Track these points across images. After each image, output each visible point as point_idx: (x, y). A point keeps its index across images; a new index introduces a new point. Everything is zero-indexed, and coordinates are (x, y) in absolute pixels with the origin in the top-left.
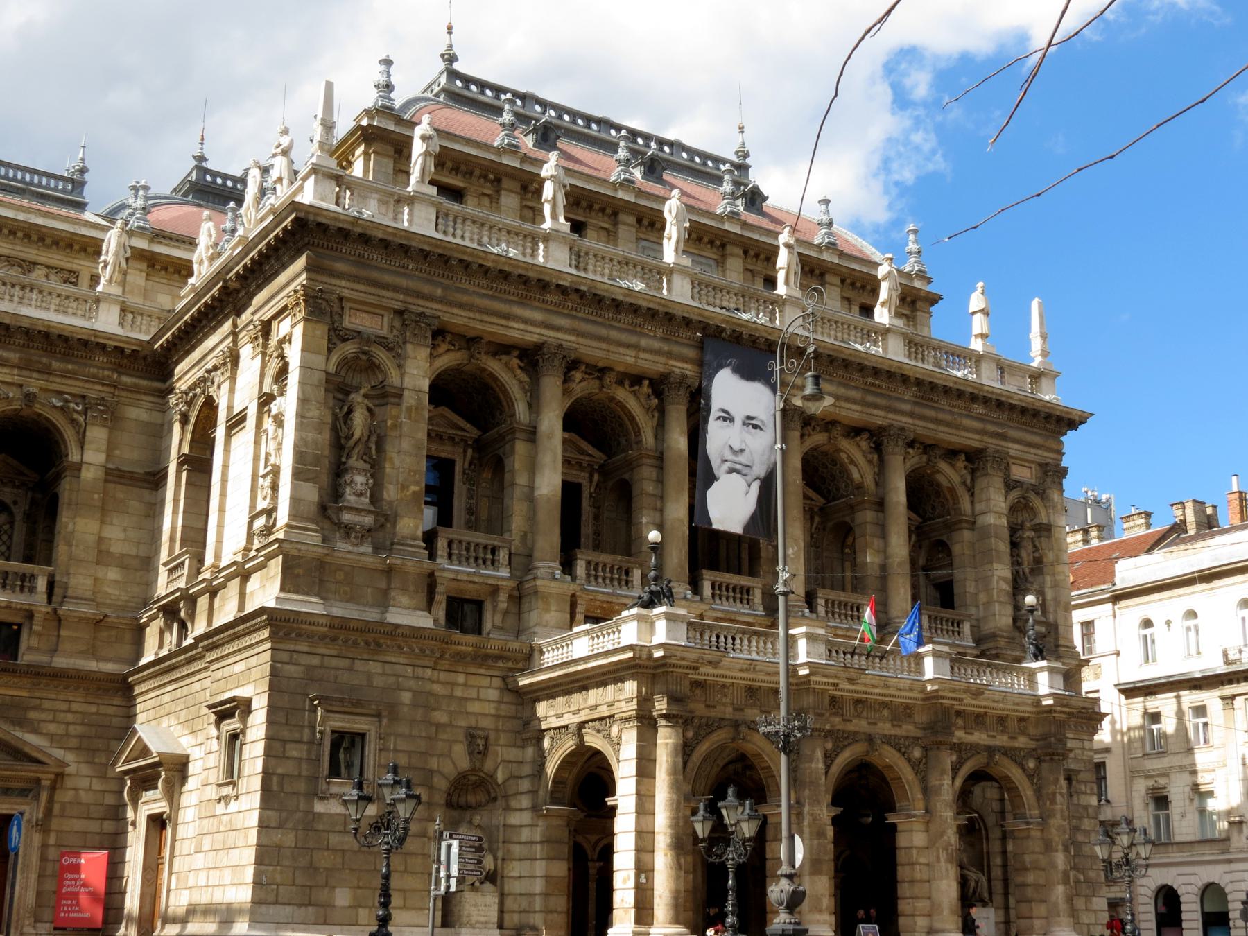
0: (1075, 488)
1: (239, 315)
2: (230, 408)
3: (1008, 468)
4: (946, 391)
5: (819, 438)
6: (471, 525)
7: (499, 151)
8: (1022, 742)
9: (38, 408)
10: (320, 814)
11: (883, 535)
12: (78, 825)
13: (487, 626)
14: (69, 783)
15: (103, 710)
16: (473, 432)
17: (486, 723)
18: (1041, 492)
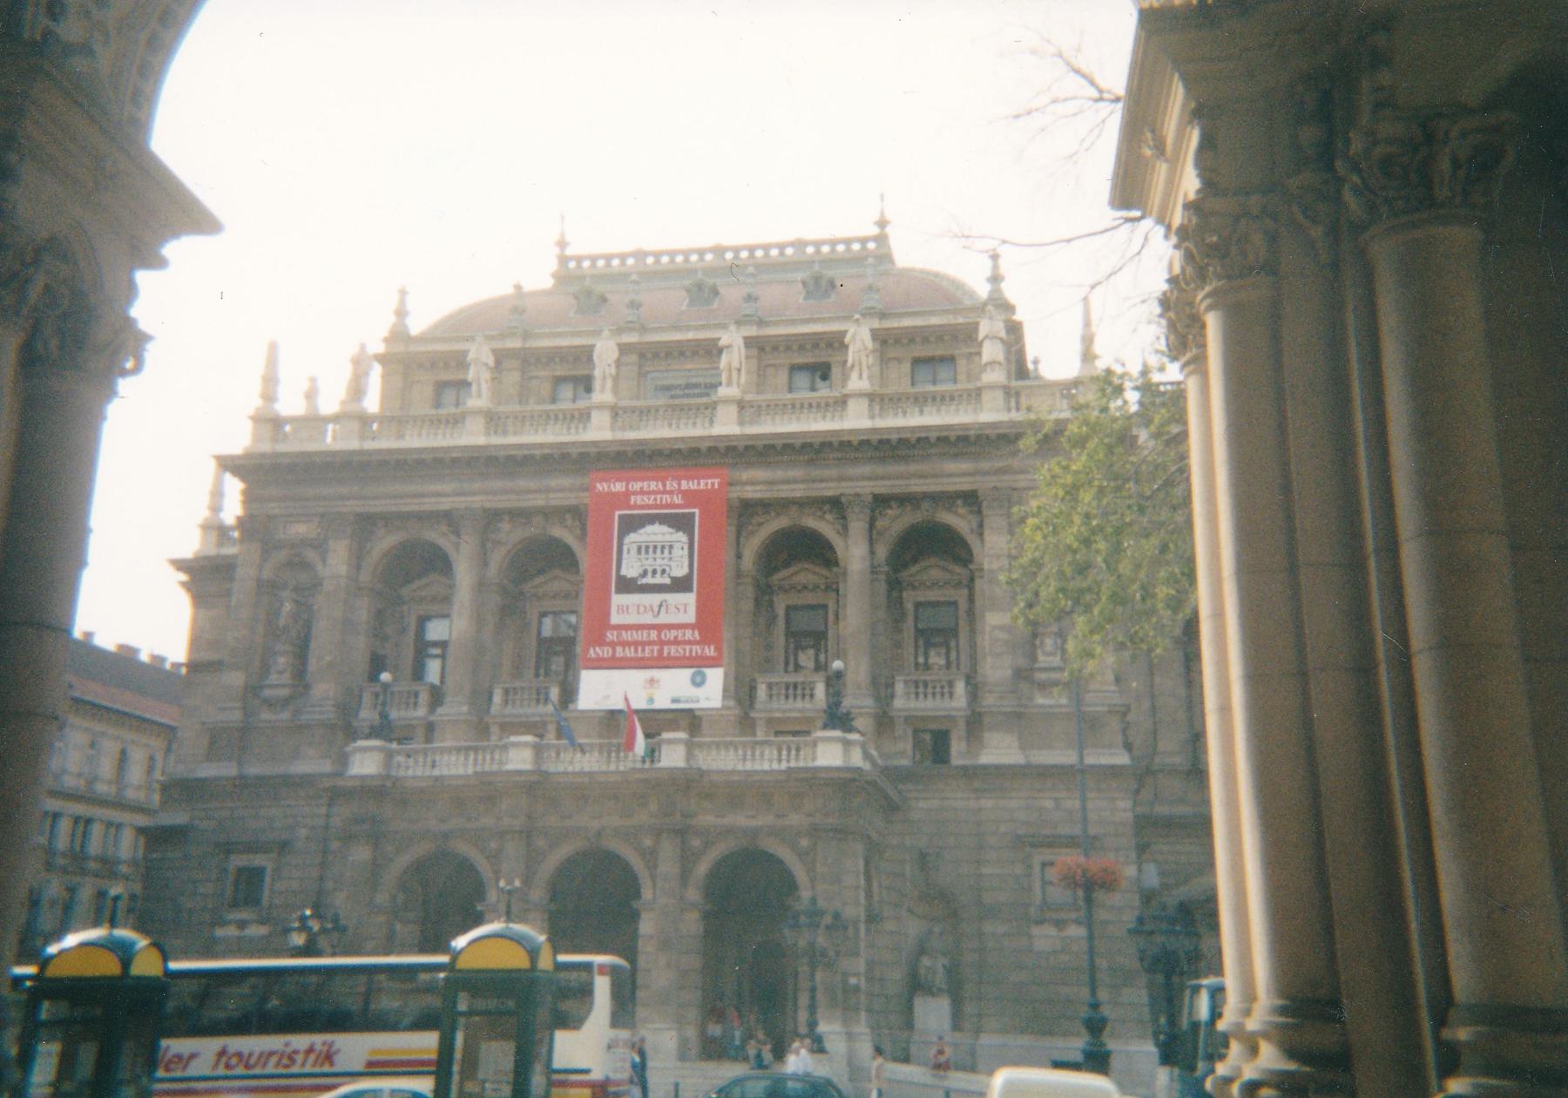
8: (795, 819)
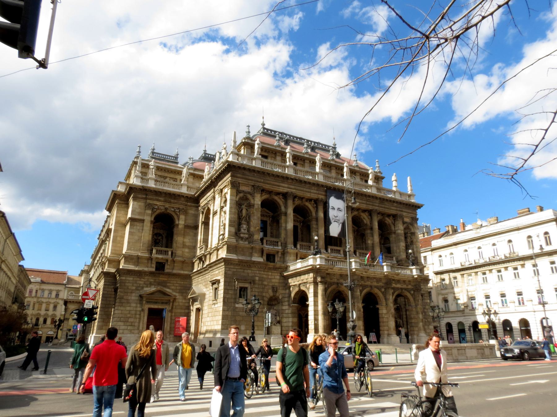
0: (420, 223)
1: (215, 187)
2: (213, 210)
3: (403, 219)
4: (387, 200)
5: (355, 213)
6: (272, 236)
7: (275, 146)
8: (410, 287)
9: (168, 211)
10: (237, 308)
11: (373, 236)
12: (179, 311)
13: (276, 261)
14: (177, 301)
15: (185, 283)
16: (271, 214)
17: (276, 284)
18: (412, 224)
